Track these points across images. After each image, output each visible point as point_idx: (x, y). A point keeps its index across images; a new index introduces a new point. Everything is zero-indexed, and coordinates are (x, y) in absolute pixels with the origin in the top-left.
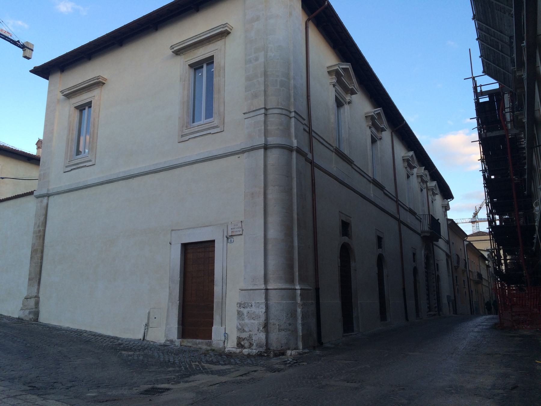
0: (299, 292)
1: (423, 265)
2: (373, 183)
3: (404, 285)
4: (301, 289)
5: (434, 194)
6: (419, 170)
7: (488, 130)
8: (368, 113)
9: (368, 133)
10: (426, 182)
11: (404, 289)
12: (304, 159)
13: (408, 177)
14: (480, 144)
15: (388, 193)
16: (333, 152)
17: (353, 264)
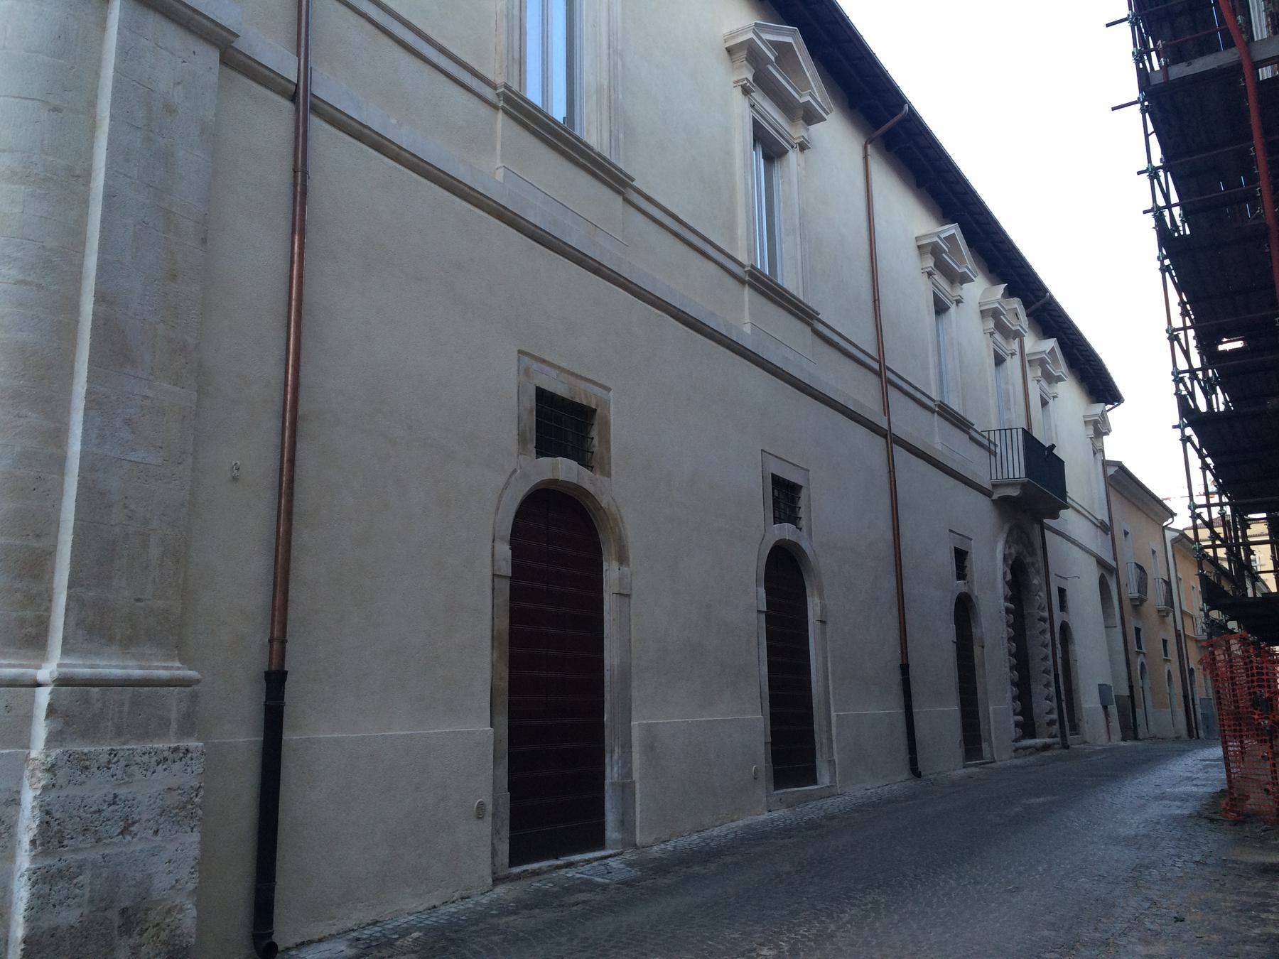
0: (43, 697)
1: (1001, 589)
2: (752, 286)
3: (278, 641)
4: (63, 682)
5: (1051, 379)
6: (979, 291)
7: (1173, 55)
8: (733, 35)
9: (737, 113)
10: (1018, 335)
11: (905, 668)
12: (213, 56)
13: (940, 308)
14: (1143, 111)
15: (836, 338)
16: (495, 107)
17: (612, 573)
